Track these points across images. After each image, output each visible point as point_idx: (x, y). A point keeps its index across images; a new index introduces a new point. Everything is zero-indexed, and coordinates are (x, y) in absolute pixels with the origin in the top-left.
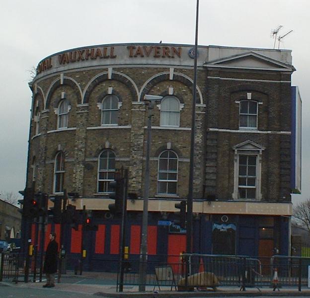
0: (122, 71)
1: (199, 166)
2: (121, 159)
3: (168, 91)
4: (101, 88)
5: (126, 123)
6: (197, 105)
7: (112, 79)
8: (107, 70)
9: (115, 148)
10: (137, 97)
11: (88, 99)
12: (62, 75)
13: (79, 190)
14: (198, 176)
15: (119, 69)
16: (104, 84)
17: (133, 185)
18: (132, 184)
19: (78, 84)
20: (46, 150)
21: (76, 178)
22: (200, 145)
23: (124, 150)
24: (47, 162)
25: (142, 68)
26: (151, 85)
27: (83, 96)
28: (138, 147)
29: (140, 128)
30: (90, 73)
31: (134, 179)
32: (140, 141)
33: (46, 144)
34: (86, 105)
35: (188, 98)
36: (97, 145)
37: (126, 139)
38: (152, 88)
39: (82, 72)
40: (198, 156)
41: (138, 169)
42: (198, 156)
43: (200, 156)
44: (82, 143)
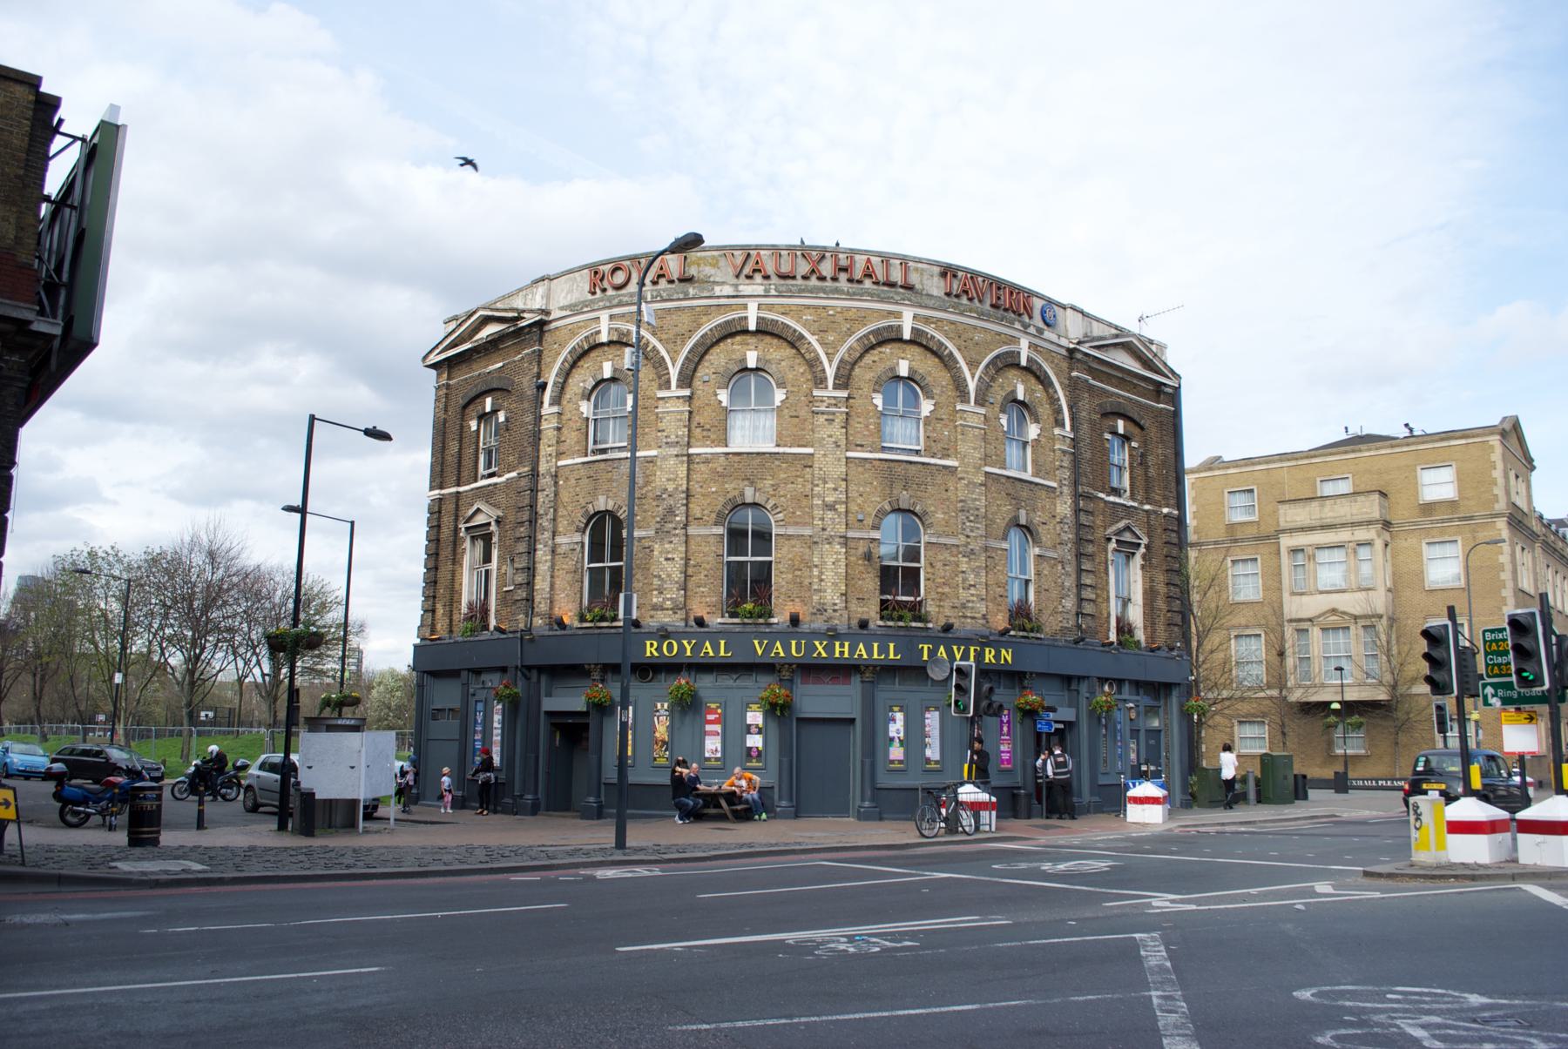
0: (933, 326)
2: (942, 540)
3: (1014, 392)
4: (881, 359)
5: (945, 452)
6: (1057, 431)
7: (911, 342)
8: (898, 315)
9: (926, 513)
10: (968, 393)
11: (849, 377)
12: (752, 306)
13: (835, 611)
15: (927, 320)
17: (970, 605)
18: (969, 601)
19: (812, 339)
20: (688, 497)
21: (822, 580)
23: (943, 519)
24: (692, 531)
25: (975, 327)
27: (830, 372)
28: (976, 513)
30: (851, 314)
31: (973, 591)
32: (979, 500)
33: (688, 481)
34: (844, 394)
35: (1044, 411)
36: (878, 499)
38: (993, 379)
39: (824, 307)
44: (835, 489)
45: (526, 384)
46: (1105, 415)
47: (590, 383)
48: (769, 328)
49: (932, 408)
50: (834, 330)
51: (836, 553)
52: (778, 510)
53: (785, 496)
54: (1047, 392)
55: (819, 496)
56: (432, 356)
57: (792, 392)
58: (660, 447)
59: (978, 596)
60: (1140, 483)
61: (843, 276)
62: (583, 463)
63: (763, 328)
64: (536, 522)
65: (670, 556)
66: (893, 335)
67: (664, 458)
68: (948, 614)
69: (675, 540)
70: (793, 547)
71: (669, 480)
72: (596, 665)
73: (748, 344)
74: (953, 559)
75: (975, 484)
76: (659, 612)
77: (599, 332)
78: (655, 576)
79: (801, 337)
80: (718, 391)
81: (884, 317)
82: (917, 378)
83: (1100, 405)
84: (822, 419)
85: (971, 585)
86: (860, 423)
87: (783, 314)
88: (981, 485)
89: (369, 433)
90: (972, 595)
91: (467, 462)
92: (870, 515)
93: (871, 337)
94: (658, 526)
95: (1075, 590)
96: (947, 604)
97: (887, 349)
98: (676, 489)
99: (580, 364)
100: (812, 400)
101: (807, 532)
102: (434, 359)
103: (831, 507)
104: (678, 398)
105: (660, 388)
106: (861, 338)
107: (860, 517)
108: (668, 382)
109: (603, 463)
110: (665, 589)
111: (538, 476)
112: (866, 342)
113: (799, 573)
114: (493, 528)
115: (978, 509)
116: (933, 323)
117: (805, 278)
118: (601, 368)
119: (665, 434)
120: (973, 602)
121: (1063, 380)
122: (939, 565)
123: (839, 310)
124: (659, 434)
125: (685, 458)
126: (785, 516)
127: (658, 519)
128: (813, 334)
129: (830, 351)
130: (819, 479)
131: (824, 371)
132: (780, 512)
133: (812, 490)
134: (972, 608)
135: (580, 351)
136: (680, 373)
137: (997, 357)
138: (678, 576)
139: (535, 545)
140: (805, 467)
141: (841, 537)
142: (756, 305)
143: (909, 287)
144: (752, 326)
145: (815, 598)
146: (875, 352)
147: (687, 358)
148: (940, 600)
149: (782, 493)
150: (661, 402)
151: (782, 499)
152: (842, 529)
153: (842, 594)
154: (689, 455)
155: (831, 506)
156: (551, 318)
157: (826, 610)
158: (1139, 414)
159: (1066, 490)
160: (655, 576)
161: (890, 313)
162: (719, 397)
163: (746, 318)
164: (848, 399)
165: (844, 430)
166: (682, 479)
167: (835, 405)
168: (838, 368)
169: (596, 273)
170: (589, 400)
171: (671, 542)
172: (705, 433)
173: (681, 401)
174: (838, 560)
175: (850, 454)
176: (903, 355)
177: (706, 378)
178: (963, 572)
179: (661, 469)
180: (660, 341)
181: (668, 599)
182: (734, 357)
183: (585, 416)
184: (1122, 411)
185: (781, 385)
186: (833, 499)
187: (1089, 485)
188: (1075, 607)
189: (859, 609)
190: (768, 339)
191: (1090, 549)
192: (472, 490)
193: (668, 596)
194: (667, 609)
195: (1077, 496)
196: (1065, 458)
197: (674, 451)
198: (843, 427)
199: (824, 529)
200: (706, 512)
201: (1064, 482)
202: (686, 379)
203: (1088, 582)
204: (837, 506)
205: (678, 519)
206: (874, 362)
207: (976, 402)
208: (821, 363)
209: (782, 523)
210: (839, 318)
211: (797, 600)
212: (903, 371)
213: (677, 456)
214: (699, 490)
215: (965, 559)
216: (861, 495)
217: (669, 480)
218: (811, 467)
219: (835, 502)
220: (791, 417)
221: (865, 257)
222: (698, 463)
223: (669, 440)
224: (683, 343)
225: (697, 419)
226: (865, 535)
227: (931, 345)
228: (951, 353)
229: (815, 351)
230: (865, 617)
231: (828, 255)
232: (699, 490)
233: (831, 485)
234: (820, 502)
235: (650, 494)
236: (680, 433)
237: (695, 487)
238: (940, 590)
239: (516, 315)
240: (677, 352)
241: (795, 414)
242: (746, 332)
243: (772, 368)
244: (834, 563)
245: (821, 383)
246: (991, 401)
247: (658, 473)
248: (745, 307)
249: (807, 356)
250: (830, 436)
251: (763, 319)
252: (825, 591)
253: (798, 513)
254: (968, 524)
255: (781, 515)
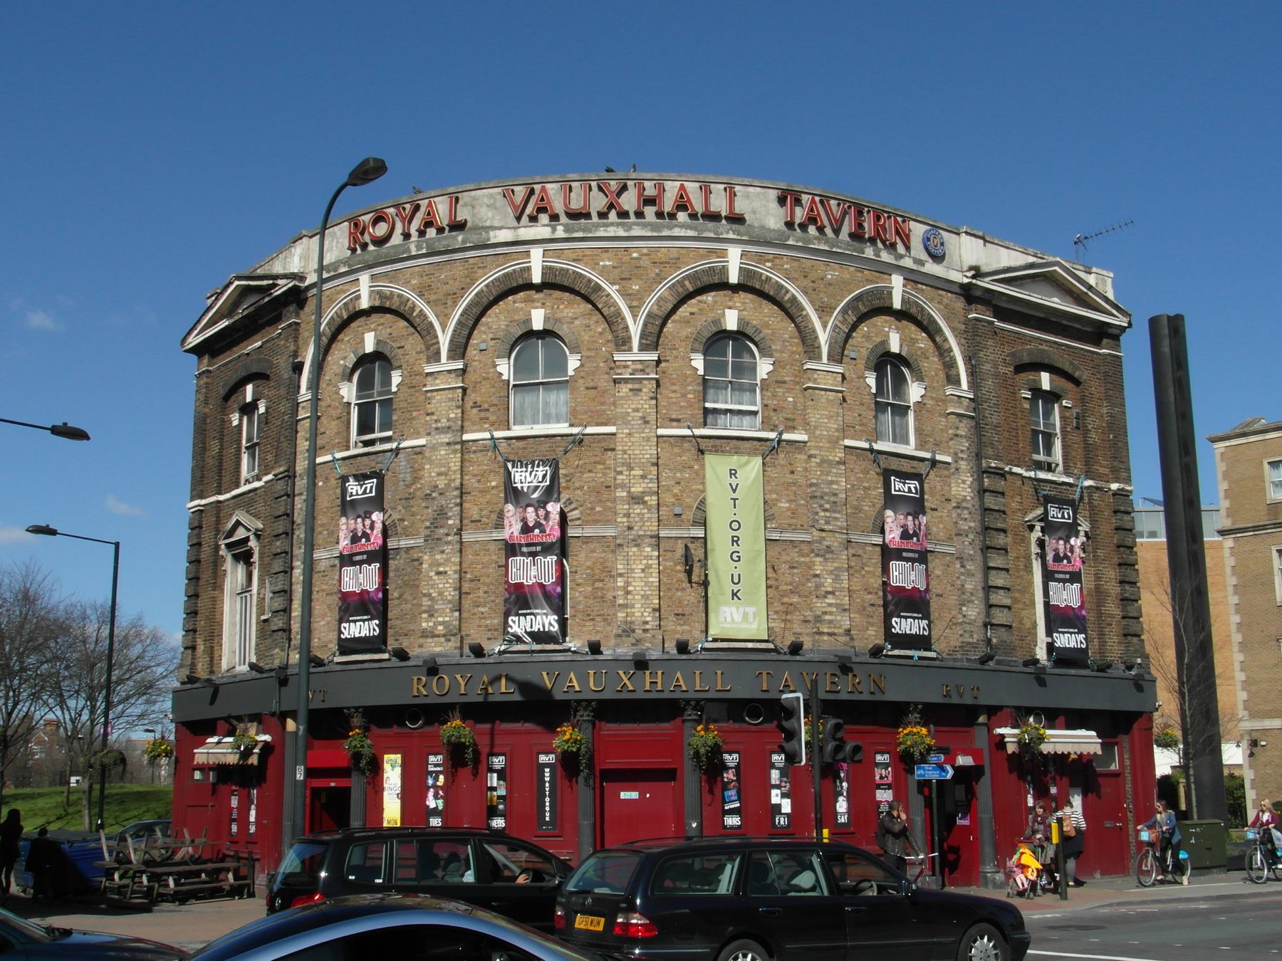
0: (769, 264)
1: (972, 567)
2: (787, 536)
3: (885, 342)
4: (700, 310)
5: (791, 424)
8: (723, 254)
10: (819, 347)
12: (536, 254)
13: (645, 631)
14: (972, 594)
16: (710, 298)
17: (827, 617)
18: (825, 613)
19: (612, 290)
21: (628, 593)
22: (970, 506)
23: (788, 509)
24: (467, 537)
26: (852, 318)
27: (635, 330)
28: (832, 499)
29: (834, 442)
30: (660, 256)
31: (830, 600)
32: (837, 483)
35: (931, 364)
37: (792, 472)
39: (626, 249)
40: (967, 536)
41: (836, 569)
42: (967, 536)
43: (971, 536)
44: (643, 477)
45: (282, 364)
46: (1020, 368)
47: (352, 359)
48: (558, 280)
49: (771, 368)
50: (639, 277)
51: (646, 557)
52: (573, 506)
53: (581, 488)
54: (934, 341)
55: (623, 486)
56: (190, 339)
57: (587, 357)
58: (429, 434)
59: (837, 605)
60: (1078, 453)
61: (650, 211)
62: (344, 459)
63: (550, 279)
64: (293, 534)
65: (441, 569)
66: (716, 280)
67: (434, 448)
68: (799, 630)
69: (448, 549)
70: (593, 551)
71: (439, 474)
72: (357, 708)
73: (533, 301)
74: (802, 559)
75: (830, 463)
76: (429, 640)
77: (358, 297)
78: (425, 595)
79: (598, 288)
80: (498, 361)
81: (703, 257)
82: (749, 331)
83: (1013, 355)
84: (625, 389)
85: (828, 593)
86: (675, 391)
87: (574, 260)
88: (839, 463)
89: (56, 431)
90: (830, 605)
91: (227, 465)
92: (691, 507)
93: (687, 283)
94: (427, 532)
95: (981, 594)
96: (796, 617)
97: (709, 298)
98: (448, 485)
99: (340, 337)
100: (613, 365)
101: (610, 532)
102: (194, 340)
103: (637, 499)
104: (449, 372)
105: (428, 362)
106: (673, 285)
107: (678, 510)
108: (438, 353)
109: (365, 458)
110: (436, 611)
111: (295, 477)
112: (680, 290)
113: (600, 585)
114: (253, 543)
115: (835, 495)
116: (768, 261)
117: (602, 215)
118: (363, 341)
119: (435, 417)
120: (831, 613)
121: (956, 324)
122: (784, 568)
123: (645, 251)
124: (428, 418)
125: (458, 447)
126: (581, 513)
127: (428, 524)
128: (613, 284)
129: (634, 304)
130: (623, 464)
131: (626, 328)
132: (575, 509)
133: (615, 479)
134: (830, 622)
135: (339, 321)
136: (451, 341)
137: (858, 298)
138: (451, 594)
139: (292, 562)
140: (606, 450)
141: (652, 537)
142: (542, 250)
143: (737, 219)
144: (537, 278)
145: (621, 615)
146: (693, 301)
147: (459, 323)
148: (787, 613)
149: (577, 485)
150: (429, 378)
151: (579, 492)
152: (652, 527)
153: (654, 610)
154: (463, 443)
155: (638, 498)
156: (307, 283)
157: (633, 631)
158: (1071, 363)
159: (963, 465)
160: (425, 595)
161: (711, 251)
162: (499, 369)
163: (529, 269)
164: (658, 362)
165: (654, 402)
166: (455, 472)
167: (641, 370)
168: (645, 325)
169: (356, 225)
170: (350, 380)
171: (443, 552)
172: (483, 414)
173: (453, 375)
174: (648, 567)
175: (661, 432)
176: (730, 304)
177: (483, 346)
178: (816, 576)
179: (430, 461)
180: (428, 303)
181: (440, 623)
182: (516, 317)
183: (345, 400)
184: (1046, 361)
185: (575, 350)
186: (641, 489)
187: (997, 458)
188: (982, 616)
189: (679, 628)
190: (557, 294)
191: (1001, 540)
192: (234, 497)
193: (440, 619)
194: (438, 636)
195: (982, 472)
196: (961, 425)
197: (445, 438)
198: (652, 398)
199: (630, 528)
200: (484, 513)
201: (961, 455)
202: (460, 348)
203: (1000, 582)
204: (646, 498)
205: (450, 522)
206: (692, 314)
207: (831, 358)
208: (623, 319)
209: (577, 523)
210: (645, 262)
211: (598, 619)
212: (731, 323)
213: (448, 444)
214: (476, 485)
215: (818, 559)
216: (678, 483)
217: (439, 474)
218: (613, 450)
219: (643, 492)
220: (587, 388)
221: (678, 184)
222: (475, 452)
223: (439, 425)
224: (455, 303)
225: (472, 397)
226: (685, 533)
227: (767, 288)
228: (794, 298)
229: (615, 304)
230: (685, 637)
231: (630, 183)
232: (476, 485)
233: (638, 472)
234: (625, 494)
235: (419, 494)
236: (452, 416)
237: (471, 482)
238: (786, 600)
239: (271, 282)
240: (447, 316)
241: (591, 385)
242: (529, 286)
243: (563, 330)
244: (643, 570)
245: (624, 343)
246: (853, 355)
247: (427, 467)
248: (527, 254)
249: (605, 311)
250: (637, 410)
251: (550, 268)
252: (633, 606)
253: (598, 509)
254: (822, 514)
255: (576, 512)
